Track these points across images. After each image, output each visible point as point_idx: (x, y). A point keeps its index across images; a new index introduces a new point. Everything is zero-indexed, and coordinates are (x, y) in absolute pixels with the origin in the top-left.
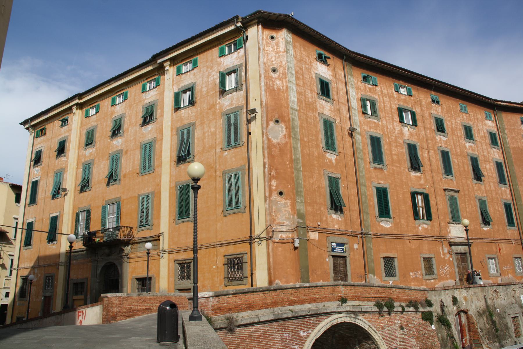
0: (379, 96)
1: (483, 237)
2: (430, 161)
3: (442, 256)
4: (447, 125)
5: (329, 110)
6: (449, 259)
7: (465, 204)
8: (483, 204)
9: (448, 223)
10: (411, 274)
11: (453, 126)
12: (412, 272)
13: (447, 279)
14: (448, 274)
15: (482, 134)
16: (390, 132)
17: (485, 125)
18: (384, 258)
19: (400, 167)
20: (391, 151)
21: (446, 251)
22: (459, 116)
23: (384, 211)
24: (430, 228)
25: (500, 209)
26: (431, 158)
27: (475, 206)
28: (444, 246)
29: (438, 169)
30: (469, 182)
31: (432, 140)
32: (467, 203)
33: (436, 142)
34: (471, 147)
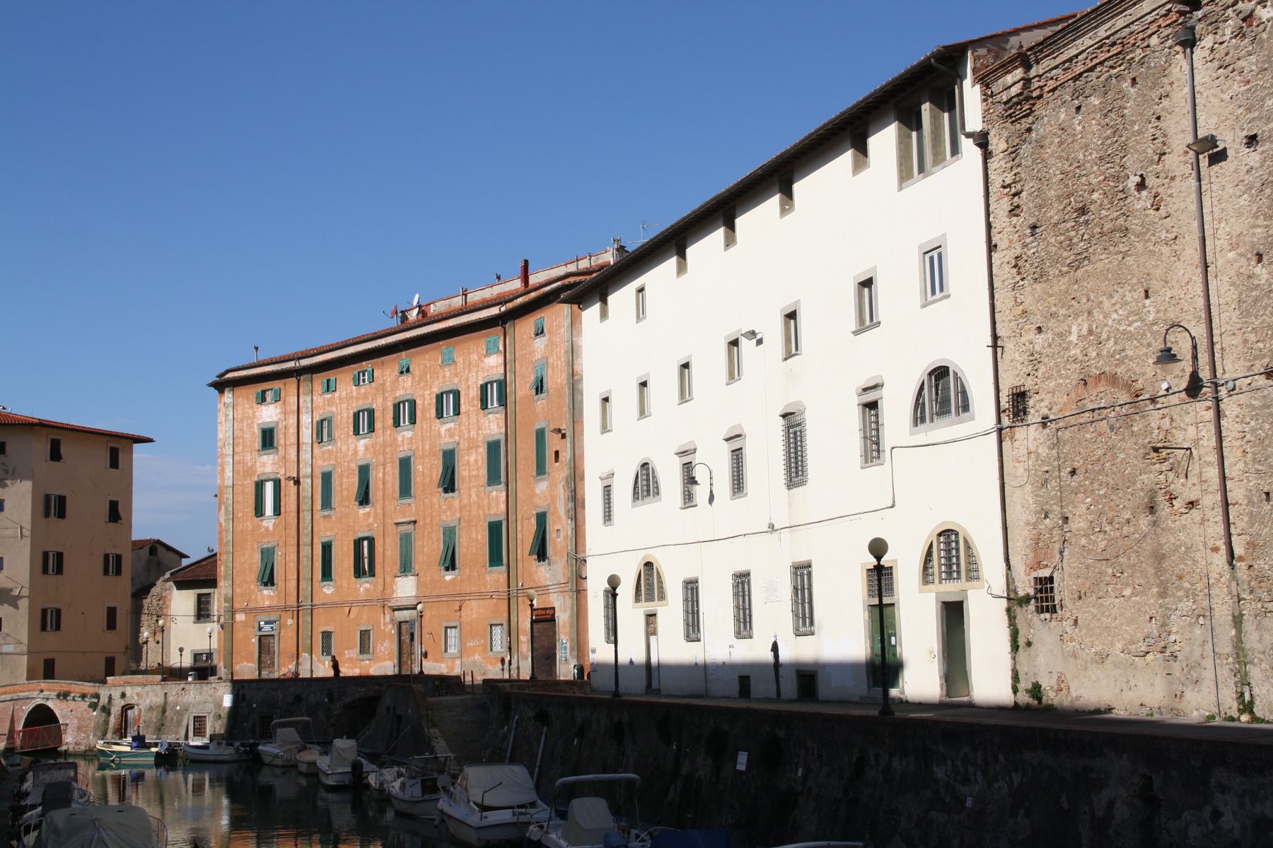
1: (443, 592)
8: (450, 533)
21: (388, 619)
27: (438, 541)
30: (435, 500)
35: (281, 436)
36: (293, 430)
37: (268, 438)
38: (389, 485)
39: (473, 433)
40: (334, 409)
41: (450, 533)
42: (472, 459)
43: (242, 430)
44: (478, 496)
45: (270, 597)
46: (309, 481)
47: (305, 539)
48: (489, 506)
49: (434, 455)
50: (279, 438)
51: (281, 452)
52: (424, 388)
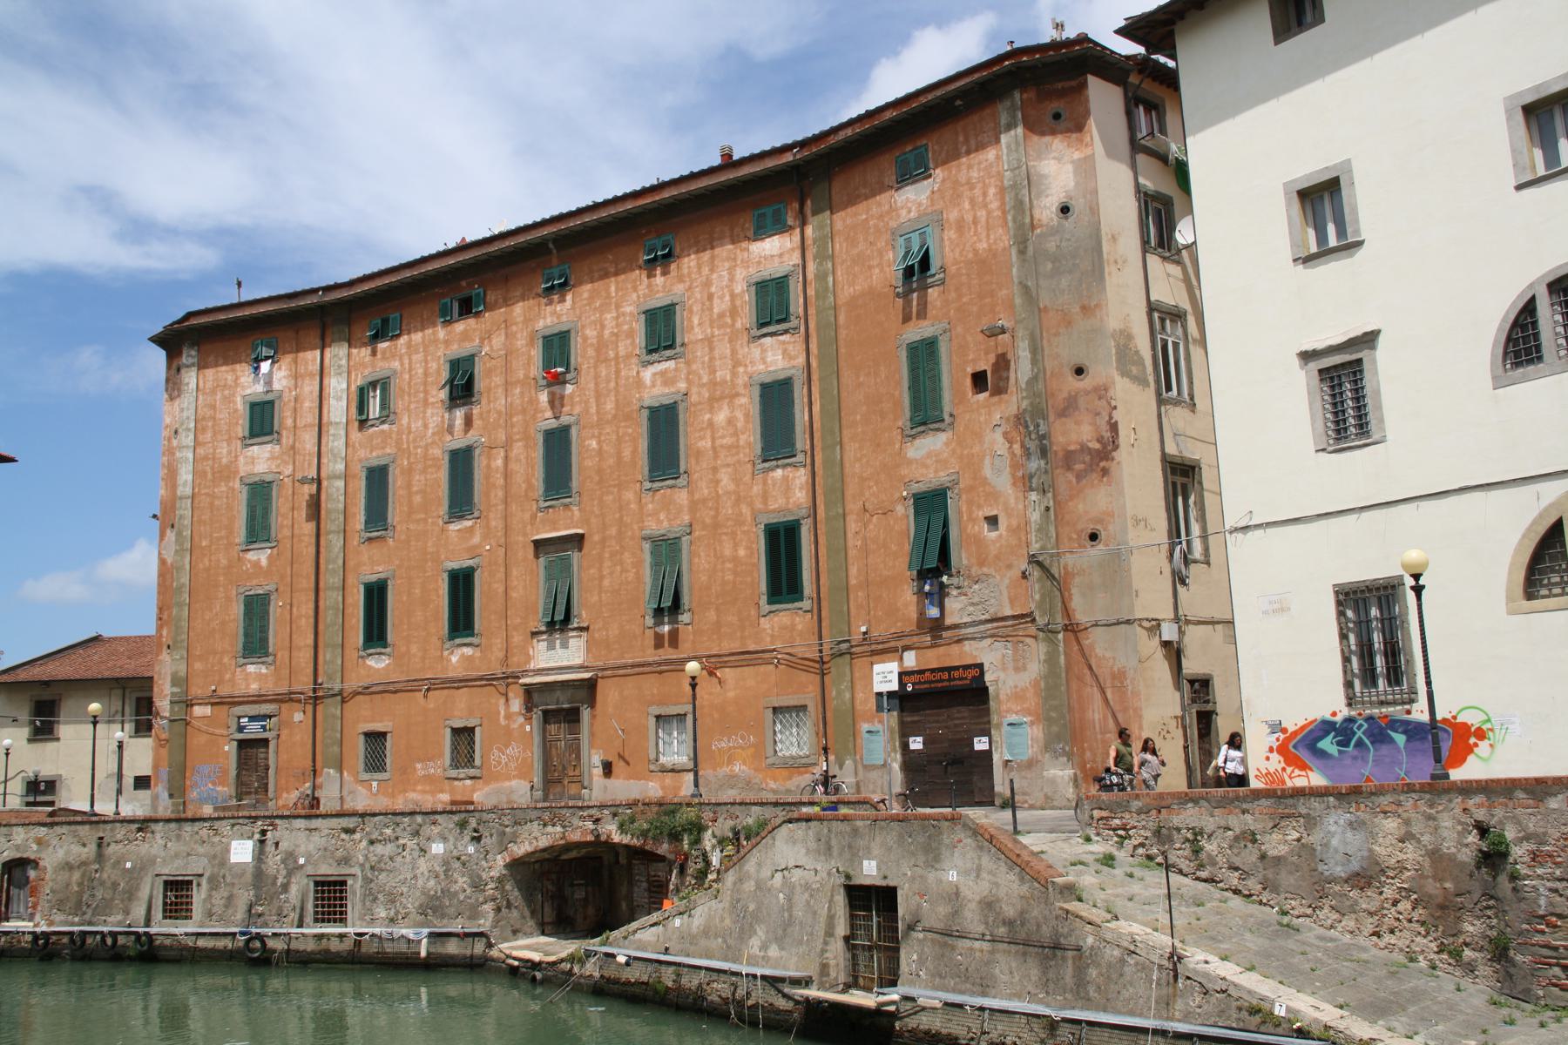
2: (507, 475)
3: (503, 722)
4: (585, 339)
6: (522, 726)
7: (600, 570)
9: (534, 634)
10: (419, 766)
11: (607, 332)
12: (420, 760)
13: (509, 778)
14: (513, 766)
15: (719, 306)
16: (415, 440)
18: (368, 735)
19: (425, 520)
20: (409, 486)
22: (635, 289)
23: (376, 633)
24: (478, 654)
25: (742, 552)
26: (513, 466)
27: (638, 564)
28: (511, 695)
29: (530, 486)
30: (629, 495)
31: (524, 411)
32: (607, 564)
33: (536, 411)
34: (663, 373)
35: (288, 414)
36: (309, 404)
37: (262, 420)
38: (519, 478)
39: (723, 374)
40: (396, 364)
41: (666, 550)
42: (721, 417)
43: (213, 407)
44: (737, 481)
45: (260, 676)
46: (341, 484)
47: (330, 579)
48: (765, 497)
49: (628, 417)
50: (283, 417)
51: (287, 439)
52: (603, 309)
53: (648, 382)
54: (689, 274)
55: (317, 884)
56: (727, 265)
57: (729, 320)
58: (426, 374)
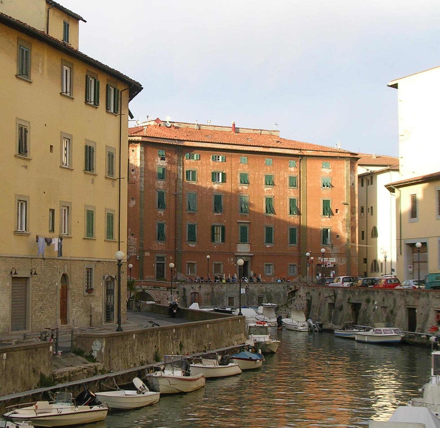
0: (199, 167)
5: (163, 185)
11: (256, 177)
15: (282, 179)
17: (287, 171)
22: (263, 169)
53: (265, 191)
54: (275, 170)
55: (258, 297)
56: (283, 170)
57: (283, 183)
58: (207, 173)
